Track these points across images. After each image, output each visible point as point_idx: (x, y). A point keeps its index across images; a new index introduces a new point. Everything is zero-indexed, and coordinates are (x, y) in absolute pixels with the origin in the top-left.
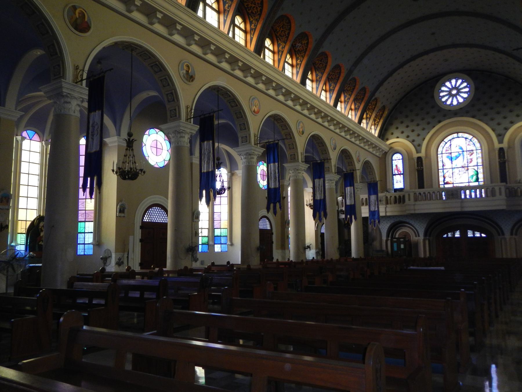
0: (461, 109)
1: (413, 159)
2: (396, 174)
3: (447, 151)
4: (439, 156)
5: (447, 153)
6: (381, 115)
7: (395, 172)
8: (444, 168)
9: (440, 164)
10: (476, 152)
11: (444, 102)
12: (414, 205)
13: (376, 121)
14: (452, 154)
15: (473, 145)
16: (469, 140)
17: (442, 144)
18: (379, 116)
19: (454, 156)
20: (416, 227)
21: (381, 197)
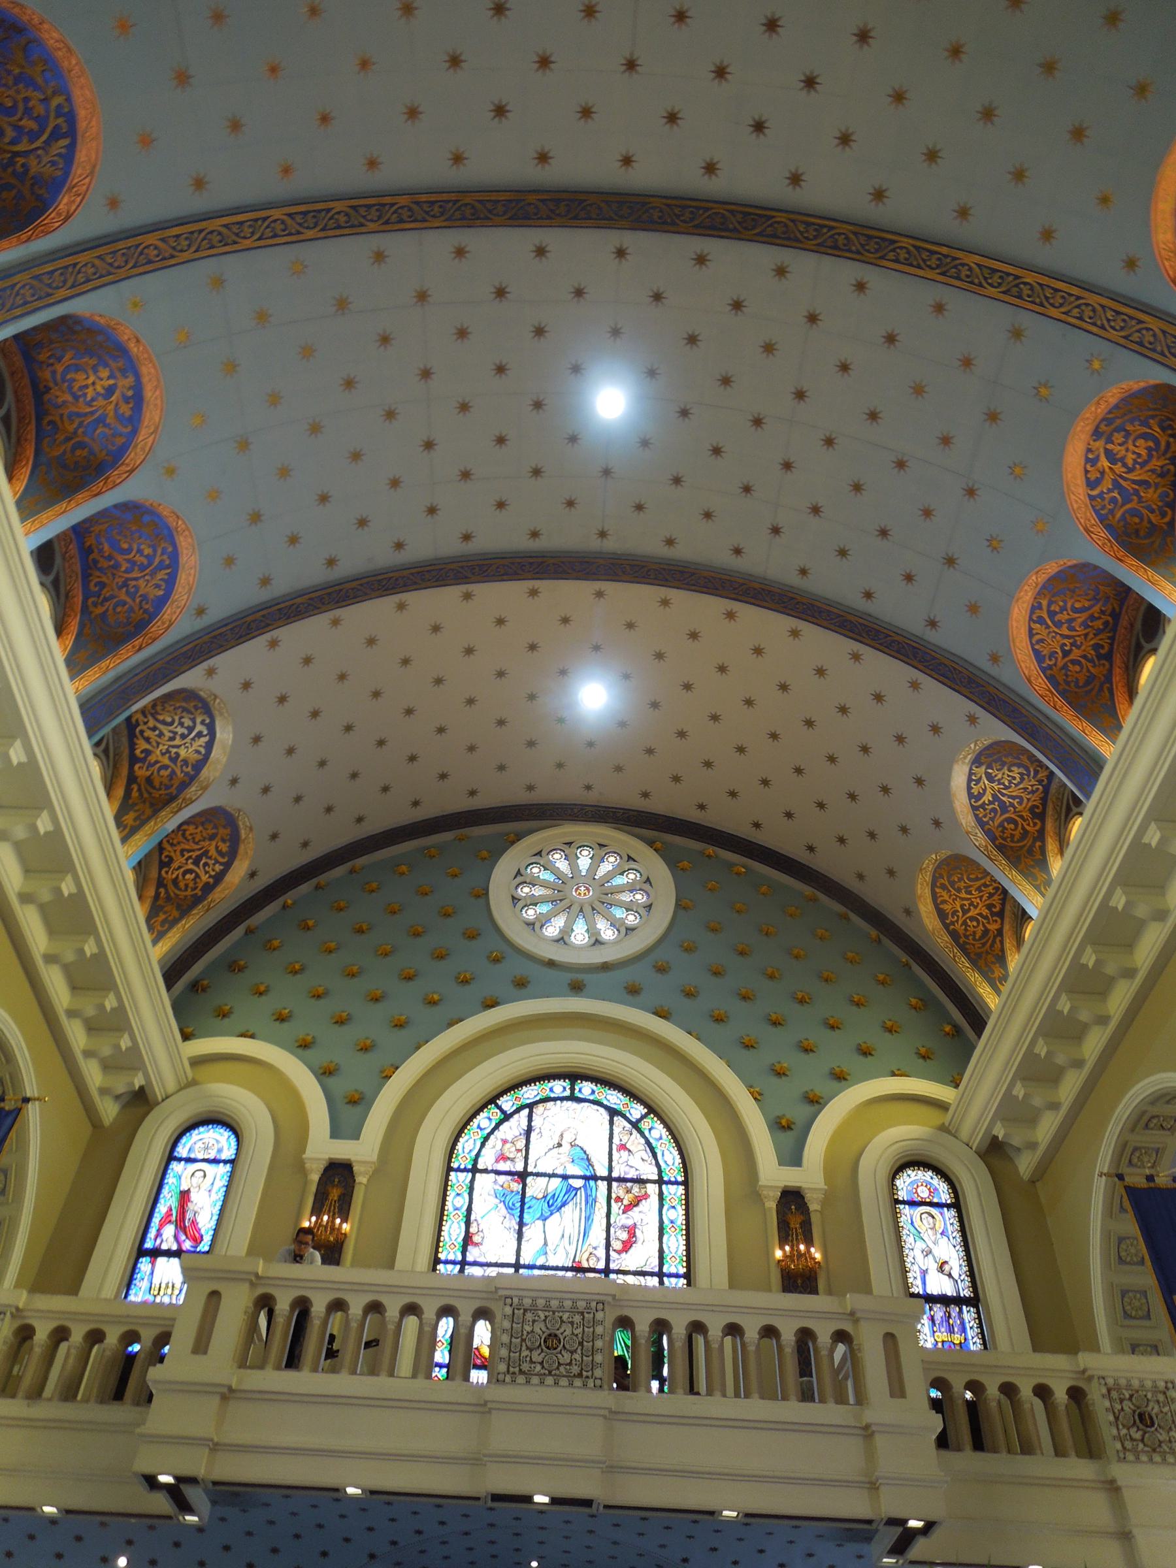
0: (605, 967)
1: (301, 1168)
2: (164, 1247)
3: (503, 1158)
4: (459, 1180)
7: (159, 1234)
8: (470, 1258)
9: (453, 1231)
10: (661, 1194)
11: (530, 924)
12: (228, 1394)
13: (162, 917)
14: (529, 1180)
15: (648, 1156)
16: (628, 1126)
17: (484, 1121)
18: (189, 892)
19: (540, 1196)
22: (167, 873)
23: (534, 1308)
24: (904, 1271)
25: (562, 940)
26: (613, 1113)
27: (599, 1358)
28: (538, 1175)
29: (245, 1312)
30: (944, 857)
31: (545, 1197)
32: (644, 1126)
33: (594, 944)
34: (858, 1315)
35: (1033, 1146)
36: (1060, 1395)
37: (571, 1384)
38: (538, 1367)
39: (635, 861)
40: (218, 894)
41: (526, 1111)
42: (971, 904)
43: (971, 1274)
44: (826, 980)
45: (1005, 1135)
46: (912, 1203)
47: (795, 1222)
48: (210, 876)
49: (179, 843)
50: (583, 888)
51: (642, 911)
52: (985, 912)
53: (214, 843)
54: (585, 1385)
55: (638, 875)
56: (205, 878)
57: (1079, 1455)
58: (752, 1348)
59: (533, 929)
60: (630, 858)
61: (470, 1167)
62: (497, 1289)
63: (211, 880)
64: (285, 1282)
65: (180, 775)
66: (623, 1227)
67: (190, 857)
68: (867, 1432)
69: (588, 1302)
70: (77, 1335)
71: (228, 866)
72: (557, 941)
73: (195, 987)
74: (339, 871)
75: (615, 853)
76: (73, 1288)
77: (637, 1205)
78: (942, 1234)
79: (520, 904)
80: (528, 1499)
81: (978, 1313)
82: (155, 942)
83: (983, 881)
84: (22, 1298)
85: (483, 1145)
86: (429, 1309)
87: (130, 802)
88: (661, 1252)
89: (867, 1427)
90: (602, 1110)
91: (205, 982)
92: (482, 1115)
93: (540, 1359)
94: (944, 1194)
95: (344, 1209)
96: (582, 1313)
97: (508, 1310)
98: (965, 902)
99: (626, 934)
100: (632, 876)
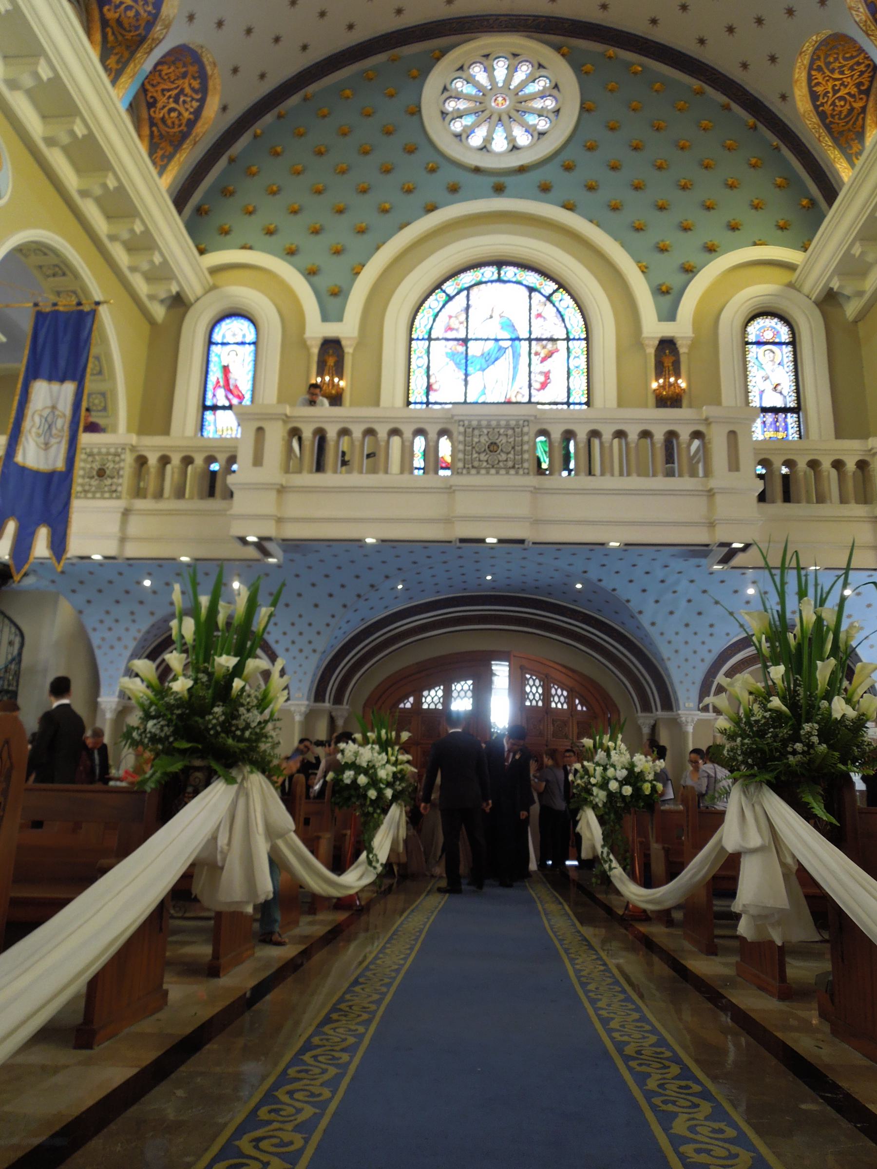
0: (522, 170)
1: (304, 345)
2: (220, 404)
4: (418, 347)
5: (447, 340)
6: (184, 128)
7: (214, 395)
10: (568, 348)
11: (458, 136)
12: (282, 490)
13: (160, 153)
14: (470, 344)
16: (544, 299)
18: (176, 130)
19: (479, 354)
20: (274, 646)
21: (108, 454)
22: (155, 112)
23: (479, 427)
24: (747, 392)
25: (484, 148)
26: (531, 290)
27: (526, 456)
28: (476, 339)
29: (283, 440)
30: (823, 37)
31: (482, 355)
32: (556, 297)
33: (511, 150)
34: (711, 420)
35: (860, 294)
36: (851, 465)
37: (507, 473)
38: (485, 464)
39: (544, 67)
40: (200, 128)
41: (465, 293)
42: (842, 84)
43: (798, 391)
44: (706, 167)
45: (839, 287)
46: (758, 343)
47: (668, 362)
48: (191, 113)
49: (159, 83)
50: (500, 99)
51: (552, 116)
52: (854, 90)
53: (186, 81)
54: (517, 473)
55: (548, 81)
56: (186, 115)
57: (857, 502)
58: (633, 445)
59: (461, 140)
60: (540, 66)
61: (426, 337)
62: (453, 416)
63: (192, 117)
64: (307, 419)
65: (145, 15)
66: (541, 373)
67: (170, 97)
68: (710, 494)
69: (517, 421)
70: (176, 460)
71: (202, 101)
72: (481, 149)
73: (199, 211)
74: (294, 100)
75: (527, 61)
76: (166, 430)
77: (550, 357)
78: (779, 364)
79: (449, 118)
80: (482, 541)
81: (799, 417)
82: (160, 174)
83: (856, 59)
84: (134, 439)
85: (434, 320)
86: (408, 432)
87: (109, 45)
88: (569, 389)
89: (710, 490)
90: (523, 288)
91: (206, 207)
92: (432, 298)
93: (485, 458)
94: (784, 334)
95: (339, 371)
96: (513, 429)
97: (462, 429)
98: (836, 83)
99: (539, 139)
100: (542, 83)
